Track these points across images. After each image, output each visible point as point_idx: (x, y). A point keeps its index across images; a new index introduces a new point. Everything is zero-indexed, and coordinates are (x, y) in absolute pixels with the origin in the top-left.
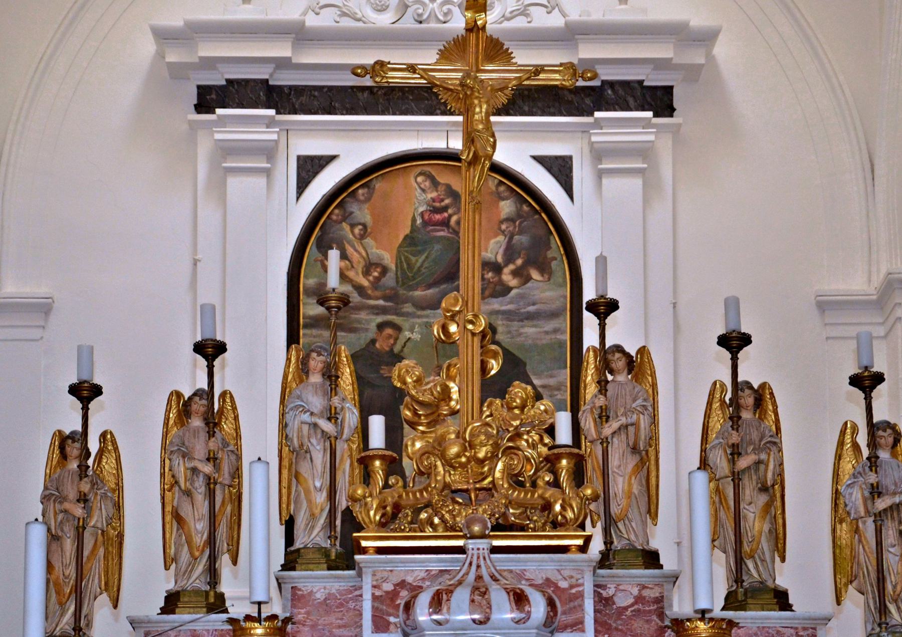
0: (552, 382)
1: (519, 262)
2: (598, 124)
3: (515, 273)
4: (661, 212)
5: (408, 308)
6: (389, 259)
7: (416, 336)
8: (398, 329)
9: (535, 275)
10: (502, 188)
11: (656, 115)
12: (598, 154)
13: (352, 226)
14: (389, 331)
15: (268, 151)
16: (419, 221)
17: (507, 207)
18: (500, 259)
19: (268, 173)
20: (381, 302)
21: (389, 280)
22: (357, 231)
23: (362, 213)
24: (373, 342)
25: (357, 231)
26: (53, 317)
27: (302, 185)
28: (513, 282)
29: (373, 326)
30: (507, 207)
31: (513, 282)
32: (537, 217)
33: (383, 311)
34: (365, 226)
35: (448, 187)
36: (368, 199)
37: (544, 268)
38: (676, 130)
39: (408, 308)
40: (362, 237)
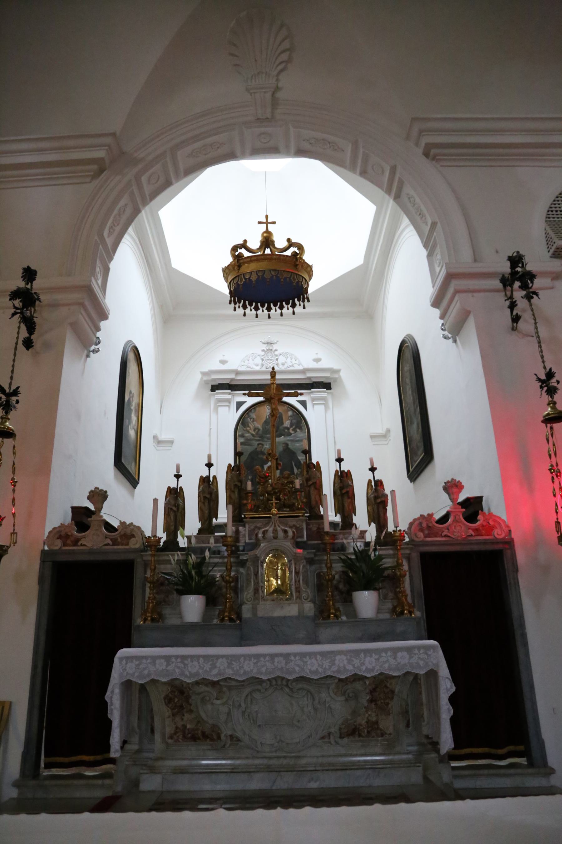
1: (294, 427)
2: (312, 392)
3: (293, 430)
4: (330, 413)
5: (265, 440)
6: (260, 427)
8: (263, 445)
9: (298, 430)
10: (289, 408)
11: (327, 390)
12: (313, 400)
13: (251, 419)
14: (260, 446)
16: (268, 417)
17: (290, 413)
18: (289, 426)
19: (229, 406)
20: (258, 438)
21: (260, 432)
22: (252, 420)
23: (253, 415)
24: (256, 448)
25: (252, 420)
27: (238, 409)
28: (292, 432)
29: (256, 444)
31: (292, 432)
32: (298, 415)
33: (259, 440)
34: (254, 419)
36: (254, 412)
37: (300, 428)
39: (265, 440)
40: (253, 422)
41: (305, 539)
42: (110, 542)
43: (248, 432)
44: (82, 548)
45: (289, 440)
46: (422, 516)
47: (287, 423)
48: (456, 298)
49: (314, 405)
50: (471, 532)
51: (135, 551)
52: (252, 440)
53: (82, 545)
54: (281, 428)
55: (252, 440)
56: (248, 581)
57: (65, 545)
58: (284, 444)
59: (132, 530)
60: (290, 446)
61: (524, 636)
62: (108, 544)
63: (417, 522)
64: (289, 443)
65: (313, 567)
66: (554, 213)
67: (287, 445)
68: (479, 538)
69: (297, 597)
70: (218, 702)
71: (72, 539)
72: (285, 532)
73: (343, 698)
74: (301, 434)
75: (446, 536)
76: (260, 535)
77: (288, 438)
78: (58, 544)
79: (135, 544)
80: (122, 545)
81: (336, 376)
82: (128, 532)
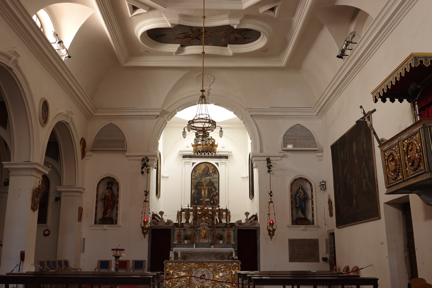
0: (216, 185)
2: (221, 160)
3: (213, 174)
5: (203, 177)
6: (201, 173)
7: (203, 180)
8: (202, 180)
9: (215, 174)
12: (221, 163)
13: (197, 169)
14: (201, 180)
15: (189, 162)
17: (212, 168)
21: (201, 175)
23: (198, 168)
26: (169, 178)
27: (193, 165)
28: (213, 175)
29: (199, 179)
30: (212, 168)
31: (213, 175)
33: (200, 178)
35: (207, 165)
36: (199, 167)
37: (216, 174)
38: (228, 160)
40: (198, 170)
41: (211, 225)
42: (165, 224)
43: (196, 174)
44: (158, 225)
45: (211, 178)
46: (239, 220)
47: (211, 172)
48: (255, 162)
49: (221, 165)
50: (250, 225)
51: (171, 227)
52: (198, 177)
53: (158, 225)
54: (209, 173)
55: (198, 177)
56: (198, 235)
57: (154, 225)
58: (209, 179)
59: (170, 221)
60: (212, 180)
61: (259, 249)
62: (165, 225)
63: (237, 222)
64: (211, 179)
65: (212, 232)
66: (286, 136)
67: (211, 180)
68: (252, 226)
69: (208, 239)
70: (192, 258)
71: (156, 223)
72: (206, 224)
73: (215, 258)
74: (216, 176)
75: (244, 225)
76: (201, 225)
77: (211, 177)
78: (152, 225)
79: (171, 225)
80: (168, 225)
81: (230, 154)
82: (170, 222)
